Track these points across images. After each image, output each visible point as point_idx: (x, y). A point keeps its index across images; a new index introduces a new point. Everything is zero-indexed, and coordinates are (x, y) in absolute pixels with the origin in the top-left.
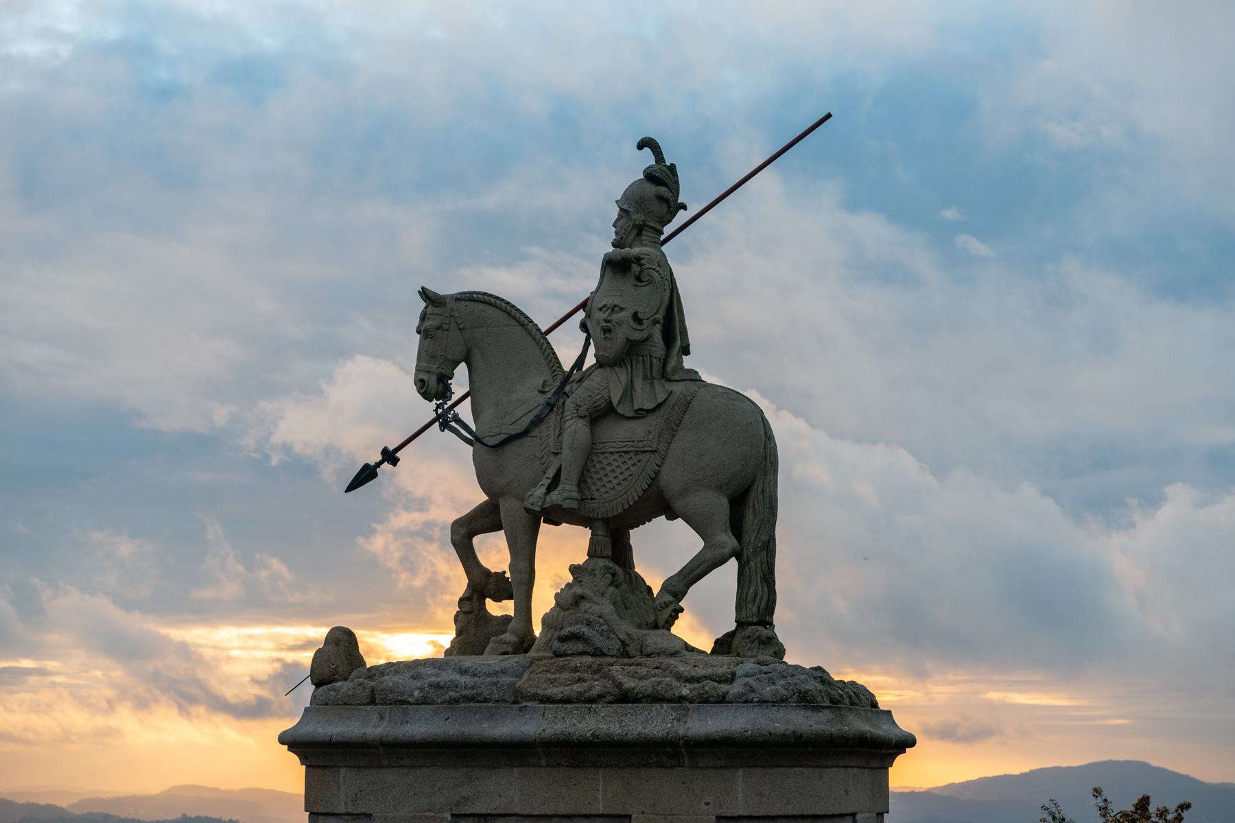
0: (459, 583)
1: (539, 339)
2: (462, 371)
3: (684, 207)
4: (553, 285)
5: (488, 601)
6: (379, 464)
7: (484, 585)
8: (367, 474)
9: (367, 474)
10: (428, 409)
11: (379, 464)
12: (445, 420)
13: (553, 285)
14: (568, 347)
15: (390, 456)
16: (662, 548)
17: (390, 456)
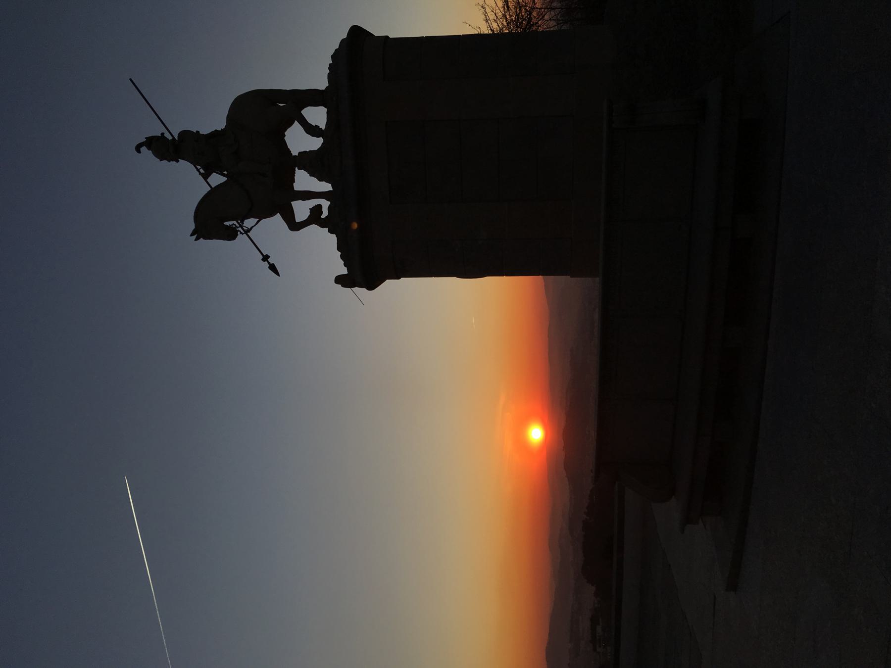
0: (314, 227)
1: (214, 191)
2: (228, 223)
3: (163, 134)
4: (190, 184)
5: (323, 216)
6: (269, 263)
7: (315, 217)
8: (273, 268)
9: (273, 268)
10: (241, 238)
11: (269, 263)
12: (247, 232)
13: (190, 184)
14: (217, 179)
15: (266, 258)
16: (299, 141)
17: (266, 258)
